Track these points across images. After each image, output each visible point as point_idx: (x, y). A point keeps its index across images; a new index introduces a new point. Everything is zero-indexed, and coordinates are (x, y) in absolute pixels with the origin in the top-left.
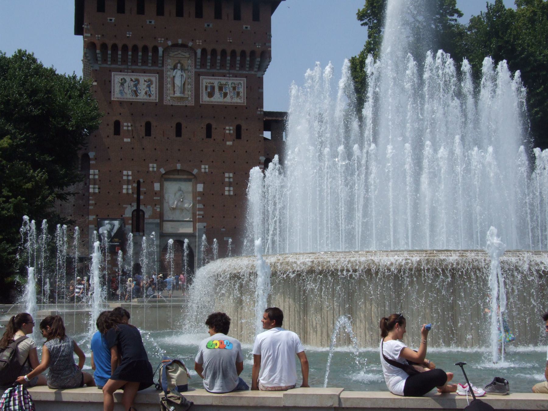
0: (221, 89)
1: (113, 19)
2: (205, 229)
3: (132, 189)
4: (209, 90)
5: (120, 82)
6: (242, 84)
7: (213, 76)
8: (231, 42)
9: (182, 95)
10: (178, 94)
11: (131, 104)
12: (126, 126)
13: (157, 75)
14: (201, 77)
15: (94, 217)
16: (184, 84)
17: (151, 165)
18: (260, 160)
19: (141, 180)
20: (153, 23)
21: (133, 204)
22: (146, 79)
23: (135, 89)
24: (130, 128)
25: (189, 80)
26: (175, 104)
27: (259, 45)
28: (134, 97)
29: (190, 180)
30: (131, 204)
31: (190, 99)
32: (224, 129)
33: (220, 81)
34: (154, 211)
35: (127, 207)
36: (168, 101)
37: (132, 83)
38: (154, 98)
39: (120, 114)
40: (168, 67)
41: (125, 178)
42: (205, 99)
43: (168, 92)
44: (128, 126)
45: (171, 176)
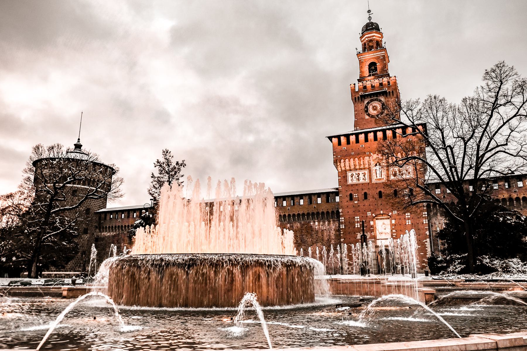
9: (380, 178)
10: (378, 178)
11: (357, 185)
15: (343, 239)
17: (368, 213)
19: (364, 221)
20: (363, 146)
22: (363, 172)
23: (358, 178)
26: (378, 182)
29: (388, 218)
34: (371, 235)
36: (374, 181)
37: (357, 175)
38: (367, 181)
39: (352, 190)
41: (356, 220)
42: (392, 178)
43: (374, 177)
44: (356, 196)
45: (379, 217)
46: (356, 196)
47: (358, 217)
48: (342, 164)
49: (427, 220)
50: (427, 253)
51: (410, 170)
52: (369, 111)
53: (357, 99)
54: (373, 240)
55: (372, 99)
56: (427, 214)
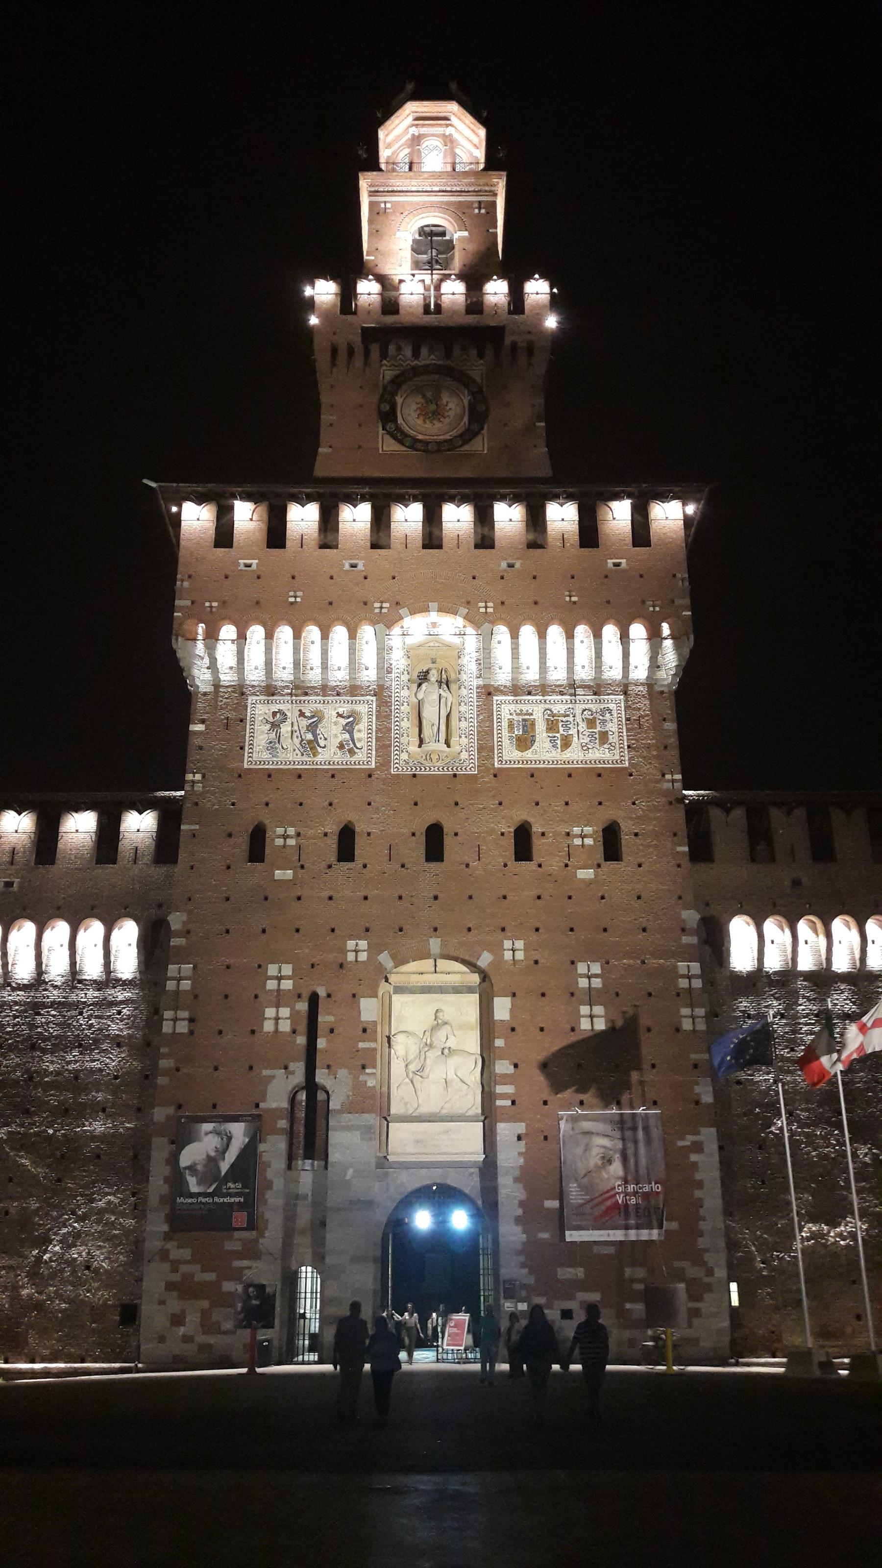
0: (552, 726)
1: (255, 562)
2: (523, 1143)
3: (291, 1017)
4: (518, 732)
5: (271, 720)
6: (615, 713)
7: (529, 693)
8: (575, 603)
12: (279, 837)
13: (374, 698)
14: (495, 698)
15: (171, 1110)
16: (448, 716)
17: (351, 944)
18: (684, 921)
19: (322, 992)
20: (360, 567)
21: (292, 1066)
23: (310, 736)
24: (291, 842)
25: (463, 708)
27: (654, 606)
28: (305, 758)
30: (286, 1068)
31: (464, 755)
32: (568, 834)
33: (547, 706)
35: (274, 1077)
37: (304, 723)
40: (403, 677)
41: (271, 985)
43: (404, 740)
44: (285, 837)
46: (285, 837)
47: (287, 970)
48: (226, 654)
49: (700, 1011)
50: (702, 1225)
51: (612, 727)
52: (400, 420)
53: (342, 355)
54: (371, 1119)
55: (423, 363)
56: (701, 976)
